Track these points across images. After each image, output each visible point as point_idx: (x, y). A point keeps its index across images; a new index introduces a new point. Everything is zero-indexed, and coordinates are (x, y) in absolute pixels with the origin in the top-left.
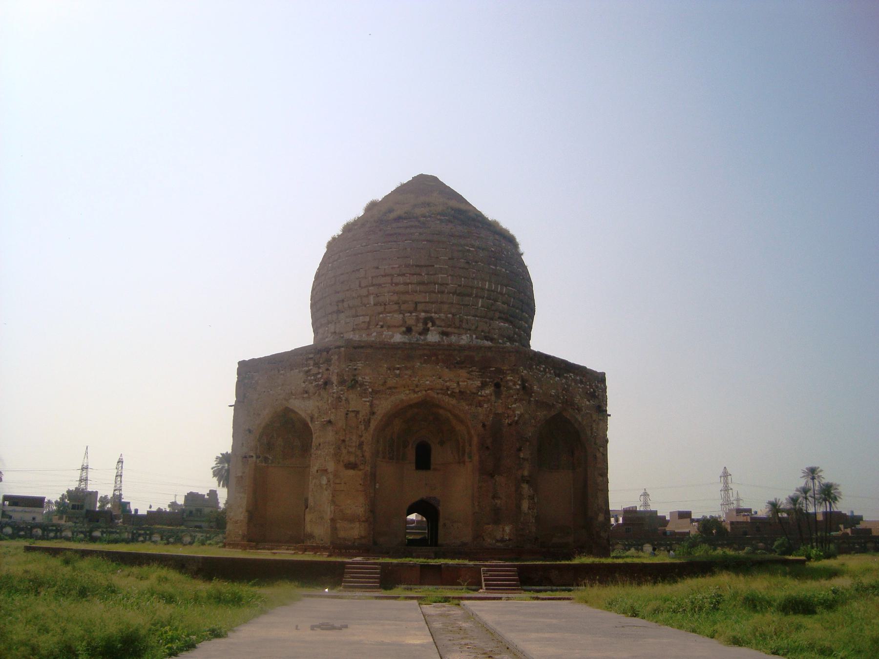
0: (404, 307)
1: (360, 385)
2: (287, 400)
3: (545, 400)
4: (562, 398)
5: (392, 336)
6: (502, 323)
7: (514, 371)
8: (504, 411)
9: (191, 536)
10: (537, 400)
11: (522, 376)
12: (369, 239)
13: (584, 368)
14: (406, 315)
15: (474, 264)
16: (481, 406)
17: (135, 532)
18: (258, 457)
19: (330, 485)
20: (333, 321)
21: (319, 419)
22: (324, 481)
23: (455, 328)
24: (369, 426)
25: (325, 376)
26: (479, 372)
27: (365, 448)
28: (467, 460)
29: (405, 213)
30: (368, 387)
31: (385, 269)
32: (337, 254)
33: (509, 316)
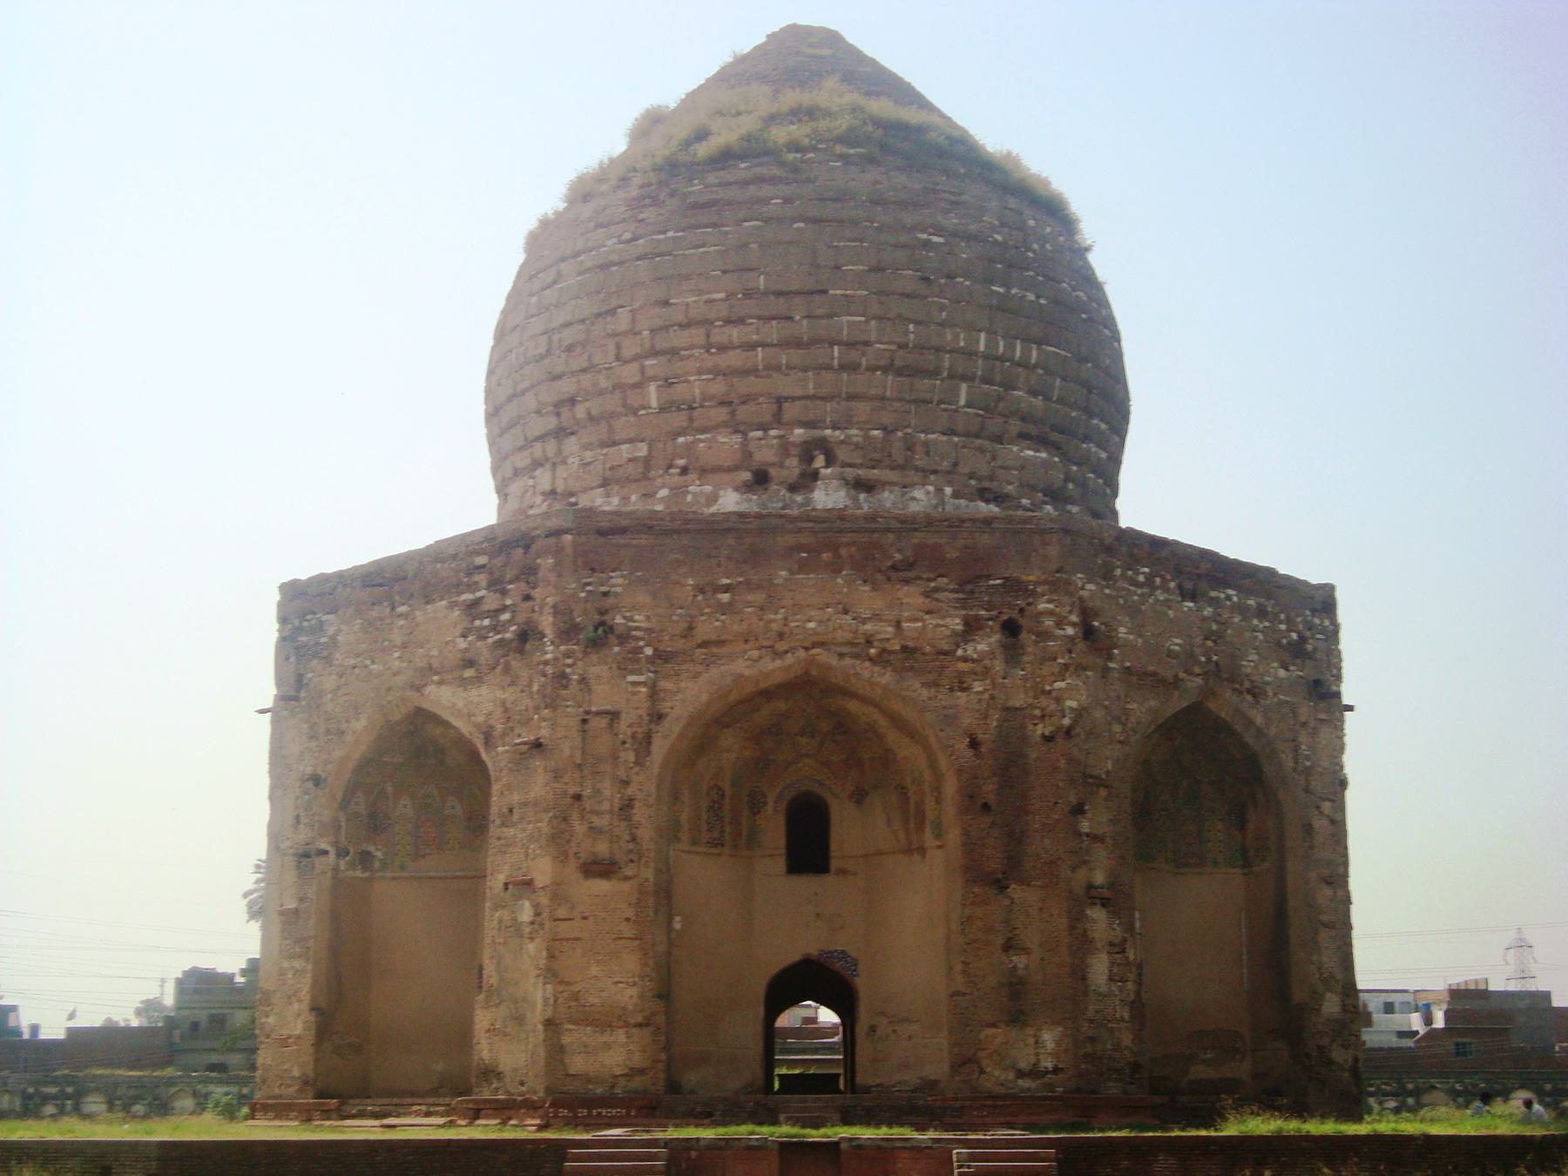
0: (743, 412)
1: (619, 637)
2: (419, 689)
3: (1151, 668)
4: (1203, 659)
5: (713, 499)
6: (1029, 449)
7: (1058, 586)
8: (1030, 700)
9: (195, 1094)
10: (1128, 668)
11: (1081, 599)
12: (642, 220)
13: (1270, 572)
15: (943, 281)
16: (965, 689)
17: (31, 1090)
18: (342, 853)
19: (542, 925)
20: (547, 459)
21: (507, 739)
22: (526, 913)
23: (892, 468)
24: (649, 753)
25: (520, 618)
26: (957, 592)
27: (640, 813)
28: (929, 840)
29: (742, 138)
30: (642, 643)
31: (687, 305)
32: (551, 266)
33: (1049, 430)
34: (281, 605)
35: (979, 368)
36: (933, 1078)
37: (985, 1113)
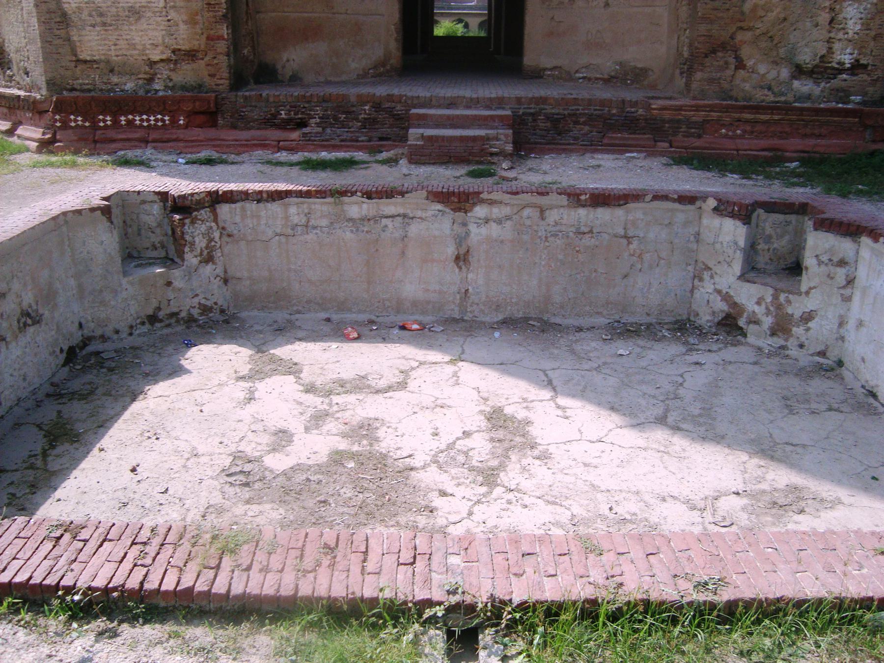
36: (640, 65)
37: (739, 132)
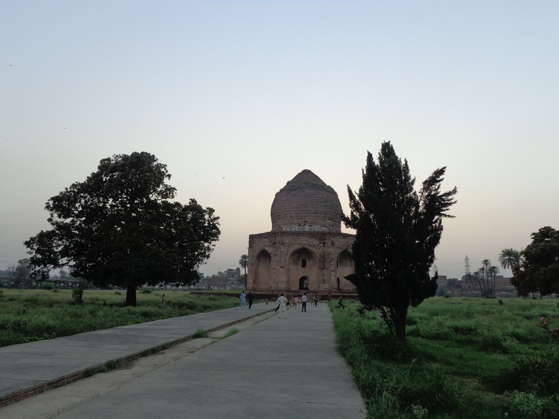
3: (339, 246)
14: (299, 220)
27: (286, 262)
34: (249, 237)
35: (323, 213)
